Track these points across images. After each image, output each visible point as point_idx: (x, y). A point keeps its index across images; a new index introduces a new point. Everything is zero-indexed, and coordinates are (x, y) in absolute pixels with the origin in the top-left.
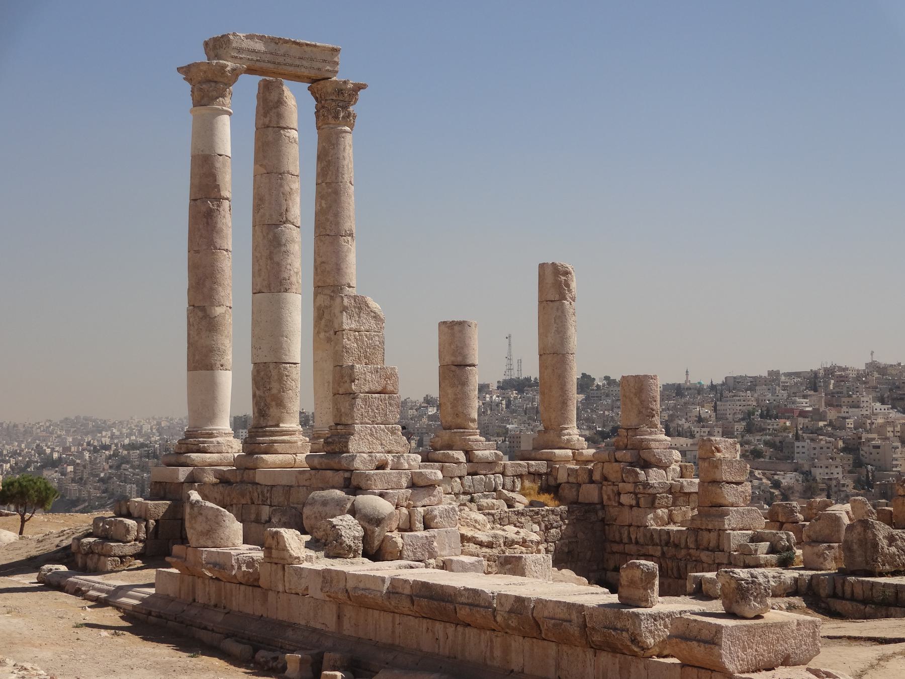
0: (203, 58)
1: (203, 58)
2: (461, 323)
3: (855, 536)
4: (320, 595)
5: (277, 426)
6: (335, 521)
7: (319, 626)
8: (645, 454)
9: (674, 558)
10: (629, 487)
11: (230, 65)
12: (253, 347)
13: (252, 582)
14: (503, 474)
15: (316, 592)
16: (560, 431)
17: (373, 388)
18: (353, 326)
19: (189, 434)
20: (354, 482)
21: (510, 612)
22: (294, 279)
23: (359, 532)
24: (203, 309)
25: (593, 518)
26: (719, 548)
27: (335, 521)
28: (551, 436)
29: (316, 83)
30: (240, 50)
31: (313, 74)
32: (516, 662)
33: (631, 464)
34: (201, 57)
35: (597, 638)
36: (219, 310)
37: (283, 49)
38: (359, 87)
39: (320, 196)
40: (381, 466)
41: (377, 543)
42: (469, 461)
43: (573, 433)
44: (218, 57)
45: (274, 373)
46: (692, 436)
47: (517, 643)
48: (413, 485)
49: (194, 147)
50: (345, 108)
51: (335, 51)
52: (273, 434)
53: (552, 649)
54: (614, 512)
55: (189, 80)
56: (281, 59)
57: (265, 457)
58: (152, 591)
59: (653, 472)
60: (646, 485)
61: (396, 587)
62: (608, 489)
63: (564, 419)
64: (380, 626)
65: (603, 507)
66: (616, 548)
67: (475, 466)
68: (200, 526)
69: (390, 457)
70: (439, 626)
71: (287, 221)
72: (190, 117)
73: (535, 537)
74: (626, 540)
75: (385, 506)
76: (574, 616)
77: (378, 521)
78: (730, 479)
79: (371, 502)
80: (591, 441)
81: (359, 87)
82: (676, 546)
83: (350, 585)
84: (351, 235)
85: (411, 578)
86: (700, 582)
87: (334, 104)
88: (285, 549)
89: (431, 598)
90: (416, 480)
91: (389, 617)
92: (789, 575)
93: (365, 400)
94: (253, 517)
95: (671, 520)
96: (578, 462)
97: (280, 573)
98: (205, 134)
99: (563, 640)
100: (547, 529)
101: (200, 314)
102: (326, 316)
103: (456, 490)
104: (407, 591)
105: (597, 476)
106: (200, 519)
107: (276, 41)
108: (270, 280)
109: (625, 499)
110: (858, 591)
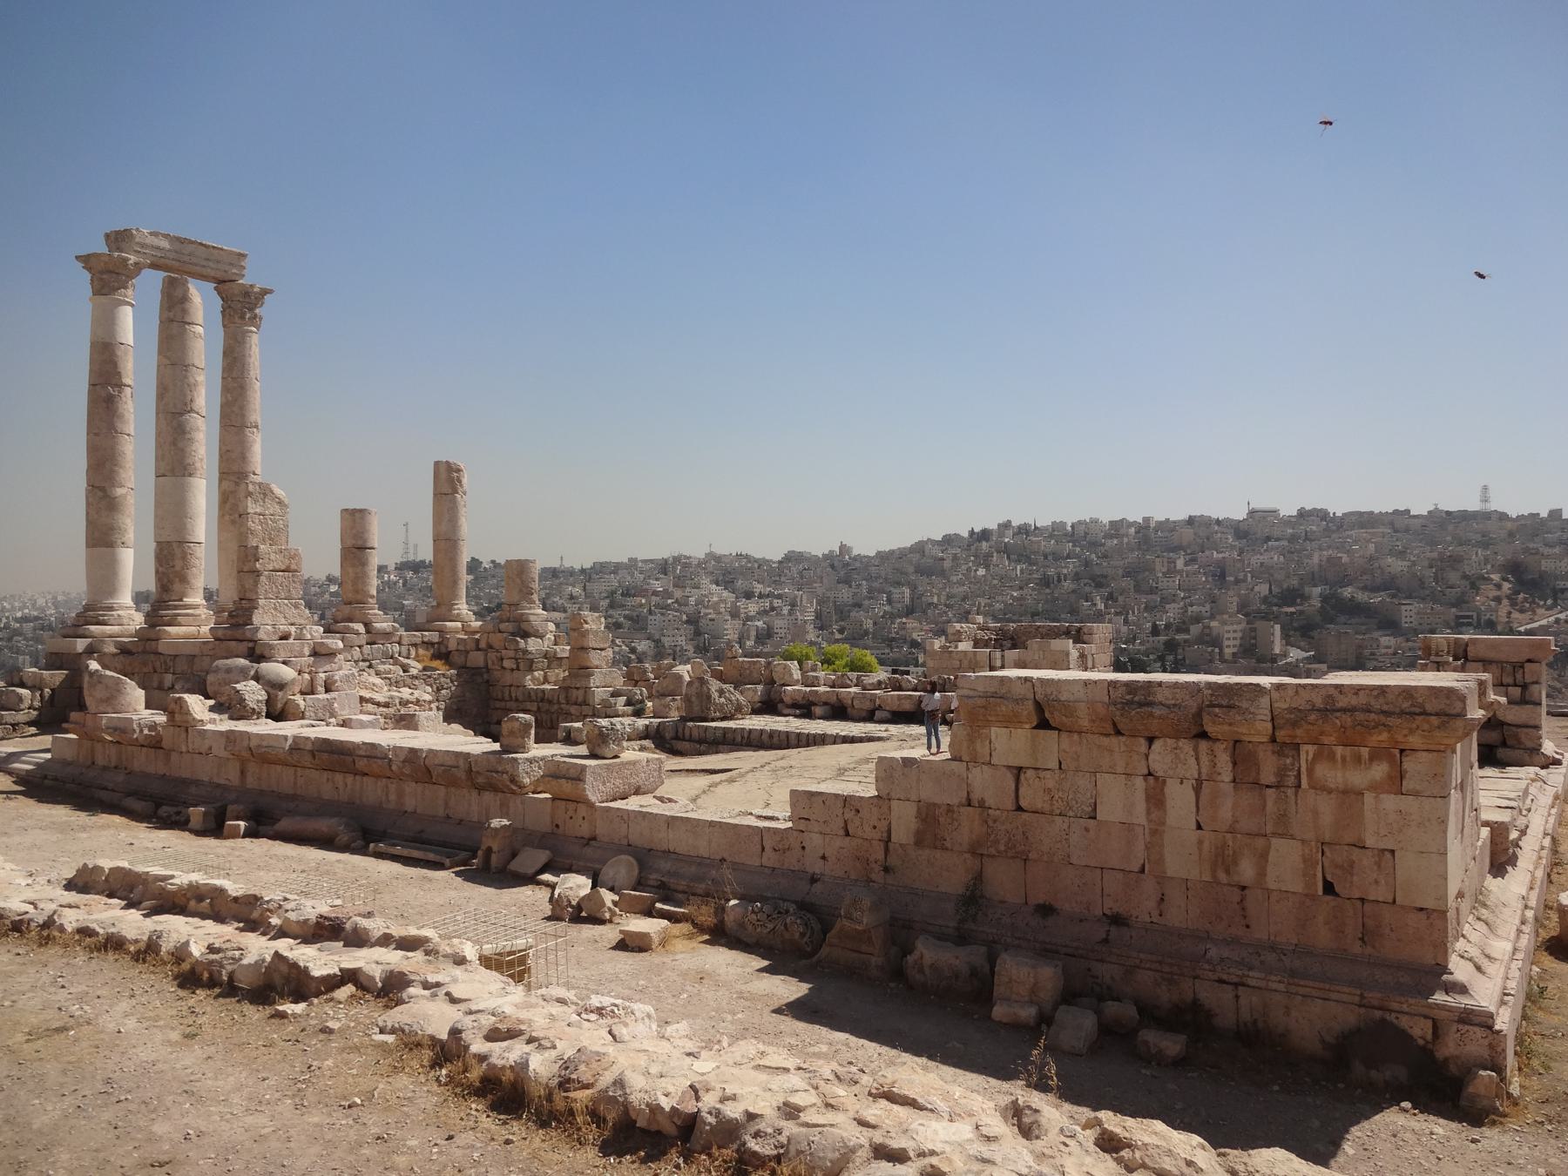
0: (104, 249)
1: (104, 249)
2: (361, 511)
3: (693, 690)
4: (223, 754)
6: (238, 686)
7: (222, 782)
8: (524, 626)
9: (547, 711)
10: (511, 653)
11: (133, 259)
12: (156, 526)
13: (154, 743)
15: (219, 751)
16: (451, 606)
19: (87, 608)
20: (258, 652)
22: (198, 465)
23: (263, 696)
24: (103, 489)
25: (479, 680)
26: (585, 703)
27: (238, 686)
28: (443, 610)
29: (223, 284)
30: (143, 246)
31: (219, 275)
32: (410, 804)
33: (513, 634)
34: (102, 248)
35: (480, 780)
36: (119, 491)
37: (191, 248)
38: (265, 292)
39: (226, 389)
40: (285, 637)
41: (280, 705)
42: (368, 632)
43: (463, 608)
44: (119, 249)
45: (178, 552)
46: (565, 611)
47: (410, 787)
48: (315, 654)
49: (93, 333)
50: (251, 310)
51: (243, 256)
52: (176, 607)
53: (442, 791)
54: (497, 674)
55: (88, 268)
56: (186, 259)
58: (48, 756)
59: (531, 641)
60: (525, 652)
61: (298, 744)
62: (492, 655)
63: (455, 596)
64: (283, 780)
65: (488, 670)
66: (498, 704)
67: (373, 636)
68: (100, 693)
69: (293, 629)
70: (339, 777)
71: (192, 410)
72: (90, 306)
73: (428, 697)
74: (507, 696)
75: (288, 673)
76: (461, 763)
77: (281, 686)
79: (274, 669)
80: (479, 615)
81: (265, 292)
82: (550, 702)
83: (253, 744)
85: (313, 736)
86: (569, 731)
87: (240, 306)
88: (188, 713)
89: (332, 752)
91: (292, 770)
92: (641, 723)
93: (269, 578)
94: (155, 684)
95: (546, 681)
96: (466, 633)
97: (183, 735)
99: (452, 782)
100: (438, 690)
101: (100, 494)
102: (231, 500)
104: (309, 746)
105: (483, 645)
106: (99, 687)
107: (178, 239)
108: (173, 463)
109: (507, 664)
110: (695, 734)
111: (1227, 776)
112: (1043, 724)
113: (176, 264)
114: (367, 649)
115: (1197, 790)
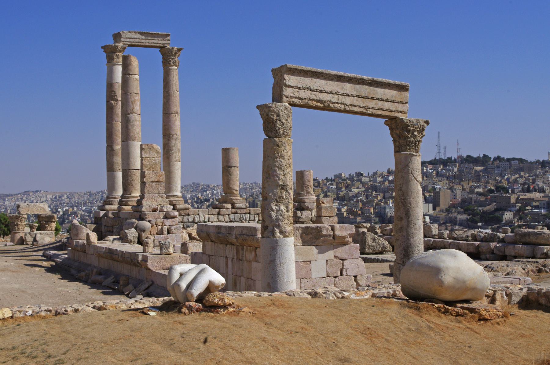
2: (228, 149)
5: (130, 194)
6: (126, 231)
14: (249, 213)
17: (153, 180)
18: (147, 156)
21: (121, 256)
22: (136, 136)
38: (179, 50)
40: (155, 210)
42: (233, 207)
49: (107, 80)
52: (128, 198)
55: (105, 51)
57: (124, 207)
58: (66, 256)
78: (325, 215)
79: (146, 224)
84: (177, 113)
90: (167, 216)
93: (149, 185)
98: (110, 74)
101: (110, 149)
103: (226, 220)
111: (235, 257)
112: (212, 241)
113: (140, 44)
114: (232, 216)
115: (232, 261)
